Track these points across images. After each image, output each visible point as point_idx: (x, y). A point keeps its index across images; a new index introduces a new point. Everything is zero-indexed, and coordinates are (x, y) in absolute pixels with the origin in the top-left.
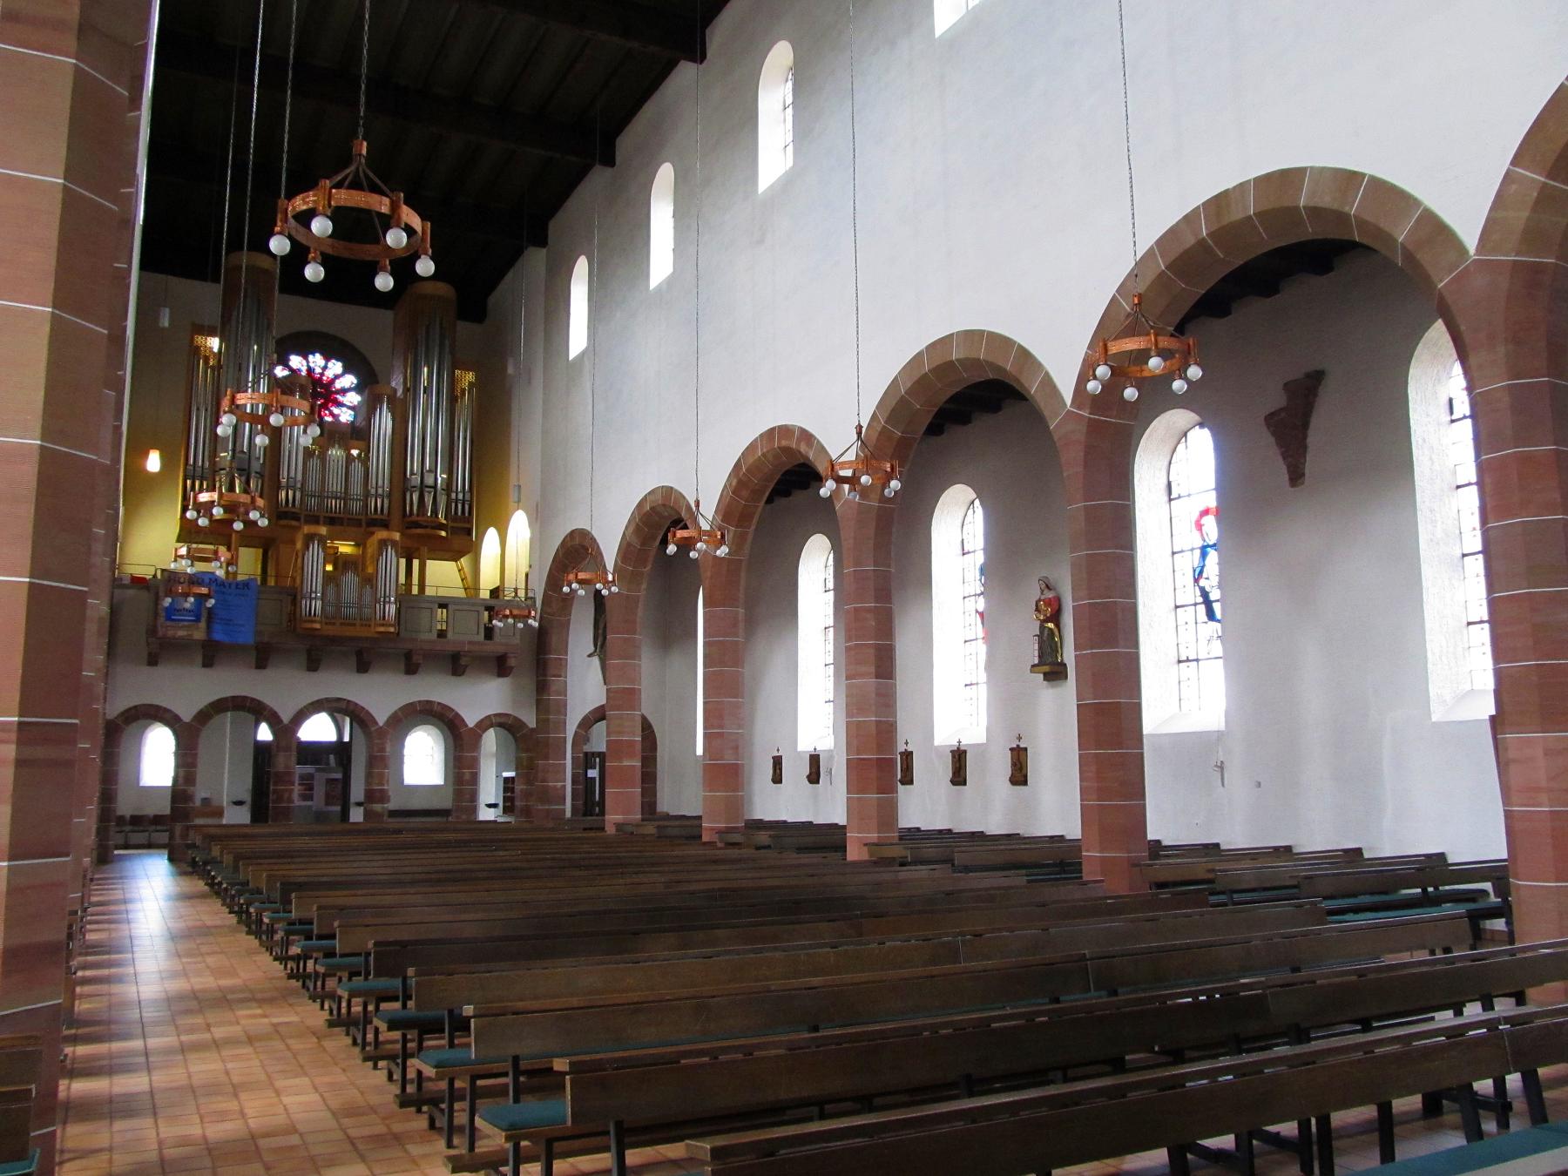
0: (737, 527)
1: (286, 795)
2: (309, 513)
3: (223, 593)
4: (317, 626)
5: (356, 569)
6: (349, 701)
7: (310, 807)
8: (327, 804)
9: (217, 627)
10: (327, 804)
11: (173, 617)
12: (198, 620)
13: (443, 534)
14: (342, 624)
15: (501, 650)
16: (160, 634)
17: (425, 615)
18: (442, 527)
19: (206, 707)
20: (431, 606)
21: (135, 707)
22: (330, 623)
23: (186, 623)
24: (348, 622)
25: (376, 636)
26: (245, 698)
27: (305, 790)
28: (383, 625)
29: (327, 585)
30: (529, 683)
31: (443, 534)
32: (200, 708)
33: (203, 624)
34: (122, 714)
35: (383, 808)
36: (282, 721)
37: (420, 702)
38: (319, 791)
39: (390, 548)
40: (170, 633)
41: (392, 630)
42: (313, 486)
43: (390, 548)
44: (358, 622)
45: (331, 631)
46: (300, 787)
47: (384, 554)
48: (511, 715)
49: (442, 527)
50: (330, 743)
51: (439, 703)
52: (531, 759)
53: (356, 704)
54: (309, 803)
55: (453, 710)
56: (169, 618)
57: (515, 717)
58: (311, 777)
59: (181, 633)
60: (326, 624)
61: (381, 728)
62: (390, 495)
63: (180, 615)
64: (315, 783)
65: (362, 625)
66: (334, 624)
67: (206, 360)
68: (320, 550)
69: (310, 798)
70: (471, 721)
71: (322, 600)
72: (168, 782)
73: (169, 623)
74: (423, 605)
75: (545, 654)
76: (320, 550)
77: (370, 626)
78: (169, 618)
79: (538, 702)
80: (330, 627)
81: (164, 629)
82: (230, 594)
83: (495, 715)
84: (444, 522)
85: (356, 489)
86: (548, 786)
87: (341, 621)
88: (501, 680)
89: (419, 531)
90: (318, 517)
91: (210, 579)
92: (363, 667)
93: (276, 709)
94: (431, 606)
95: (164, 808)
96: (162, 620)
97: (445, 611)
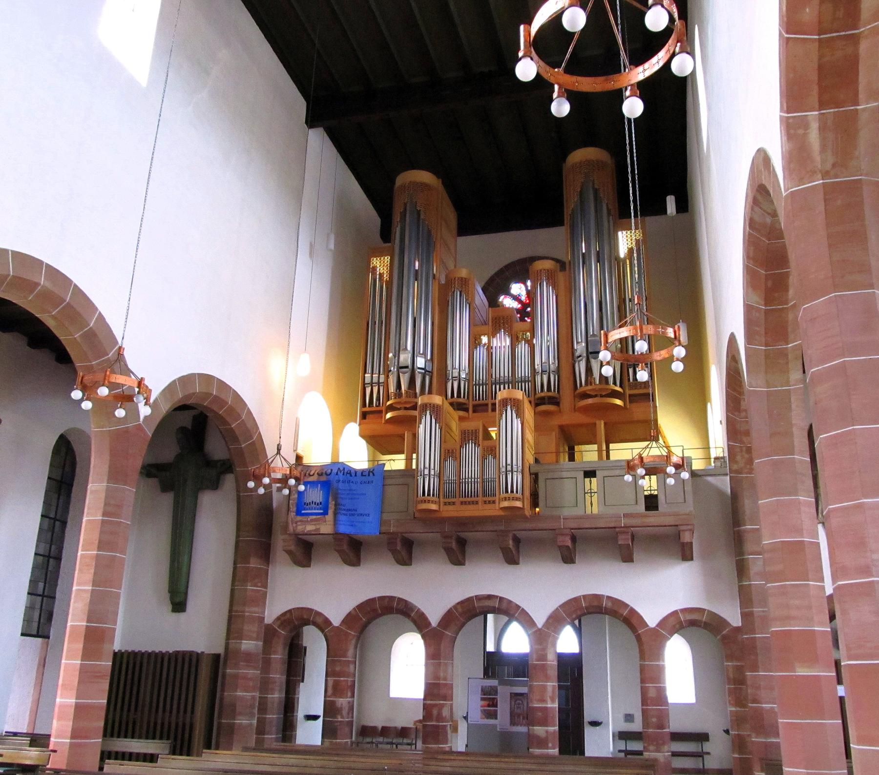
0: (822, 105)
1: (435, 712)
2: (477, 402)
3: (349, 482)
4: (434, 507)
5: (476, 437)
6: (501, 599)
7: (495, 726)
8: (513, 723)
9: (342, 518)
10: (513, 723)
11: (303, 512)
12: (325, 513)
13: (618, 402)
14: (462, 503)
15: (669, 520)
16: (291, 529)
17: (568, 485)
18: (615, 394)
19: (354, 609)
20: (573, 474)
21: (290, 611)
22: (449, 503)
23: (314, 517)
24: (469, 499)
25: (502, 513)
26: (391, 598)
27: (489, 706)
28: (505, 499)
29: (445, 460)
30: (725, 564)
31: (618, 402)
32: (347, 611)
33: (330, 517)
34: (278, 618)
35: (547, 732)
36: (430, 624)
37: (584, 596)
38: (503, 708)
39: (509, 408)
40: (300, 528)
41: (518, 504)
42: (480, 375)
43: (509, 408)
44: (480, 499)
45: (450, 511)
46: (483, 703)
47: (504, 416)
48: (704, 610)
49: (615, 394)
50: (574, 654)
51: (609, 598)
52: (740, 670)
53: (510, 602)
54: (492, 722)
55: (627, 605)
56: (298, 513)
57: (708, 611)
58: (494, 691)
59: (310, 528)
60: (445, 504)
61: (539, 630)
62: (558, 371)
63: (310, 509)
64: (499, 697)
65: (485, 502)
66: (454, 503)
67: (381, 275)
68: (434, 421)
69: (492, 715)
70: (652, 617)
71: (439, 477)
72: (421, 696)
73: (299, 518)
74: (565, 474)
75: (739, 526)
76: (434, 421)
77: (494, 502)
78: (298, 513)
79: (741, 588)
80: (451, 508)
81: (294, 525)
82: (356, 483)
83: (684, 610)
84: (618, 389)
85: (523, 370)
86: (762, 708)
87: (461, 499)
88: (687, 565)
89: (590, 401)
90: (487, 405)
91: (339, 469)
92: (512, 560)
93: (423, 610)
94: (573, 474)
95: (410, 718)
96: (292, 514)
97: (594, 480)
